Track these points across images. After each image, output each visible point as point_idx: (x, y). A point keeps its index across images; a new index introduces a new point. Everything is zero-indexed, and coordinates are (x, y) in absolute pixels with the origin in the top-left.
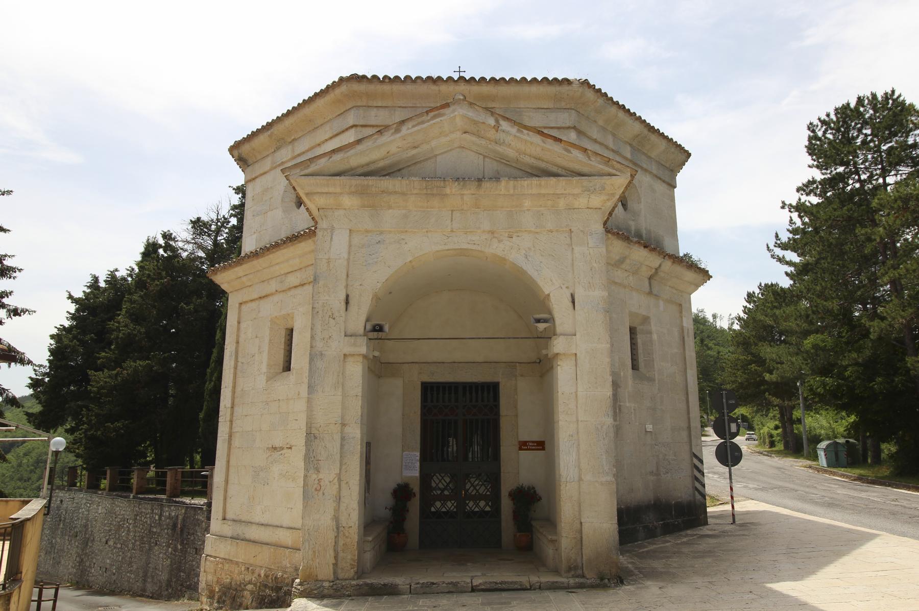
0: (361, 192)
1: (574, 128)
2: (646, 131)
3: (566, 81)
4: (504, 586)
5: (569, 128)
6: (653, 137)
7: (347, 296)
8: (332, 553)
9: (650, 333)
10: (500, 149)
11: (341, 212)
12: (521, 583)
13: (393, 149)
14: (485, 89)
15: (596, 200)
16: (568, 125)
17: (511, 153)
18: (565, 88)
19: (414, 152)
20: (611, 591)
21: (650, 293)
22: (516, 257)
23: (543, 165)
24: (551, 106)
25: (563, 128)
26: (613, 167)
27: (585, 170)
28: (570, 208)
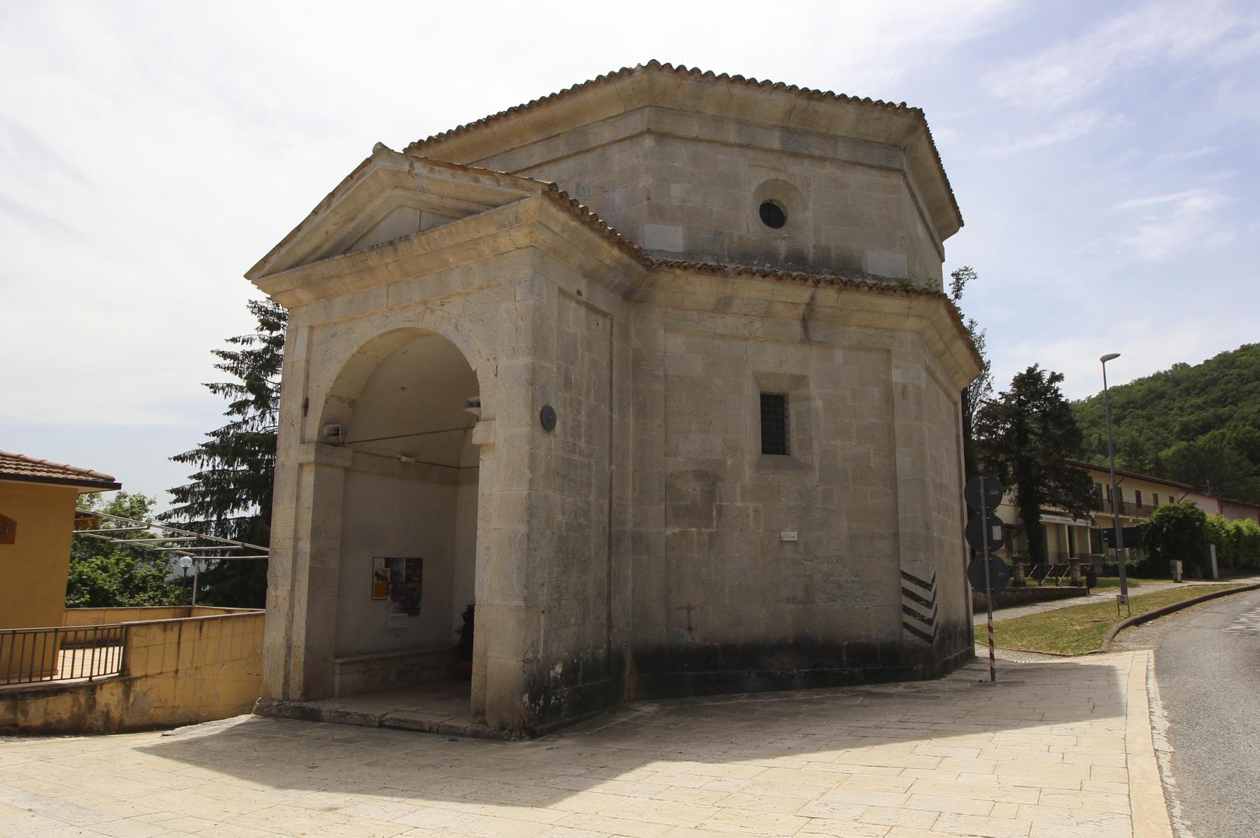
0: (307, 284)
1: (649, 131)
2: (802, 102)
3: (625, 72)
4: (406, 725)
5: (642, 134)
6: (822, 107)
7: (307, 401)
8: (281, 673)
9: (808, 399)
10: (425, 197)
11: (304, 309)
12: (420, 723)
13: (330, 226)
14: (538, 114)
15: (520, 236)
16: (639, 130)
17: (434, 199)
18: (626, 82)
19: (352, 225)
20: (511, 744)
21: (806, 339)
22: (446, 330)
23: (464, 205)
24: (622, 110)
25: (636, 136)
26: (523, 188)
27: (498, 199)
28: (499, 254)
